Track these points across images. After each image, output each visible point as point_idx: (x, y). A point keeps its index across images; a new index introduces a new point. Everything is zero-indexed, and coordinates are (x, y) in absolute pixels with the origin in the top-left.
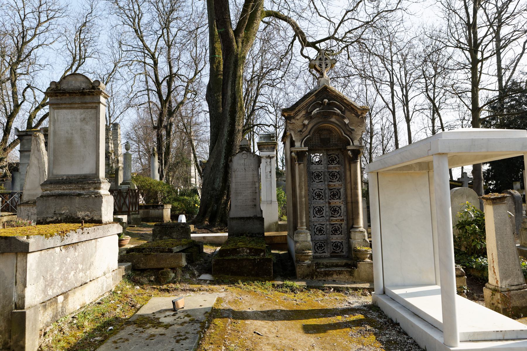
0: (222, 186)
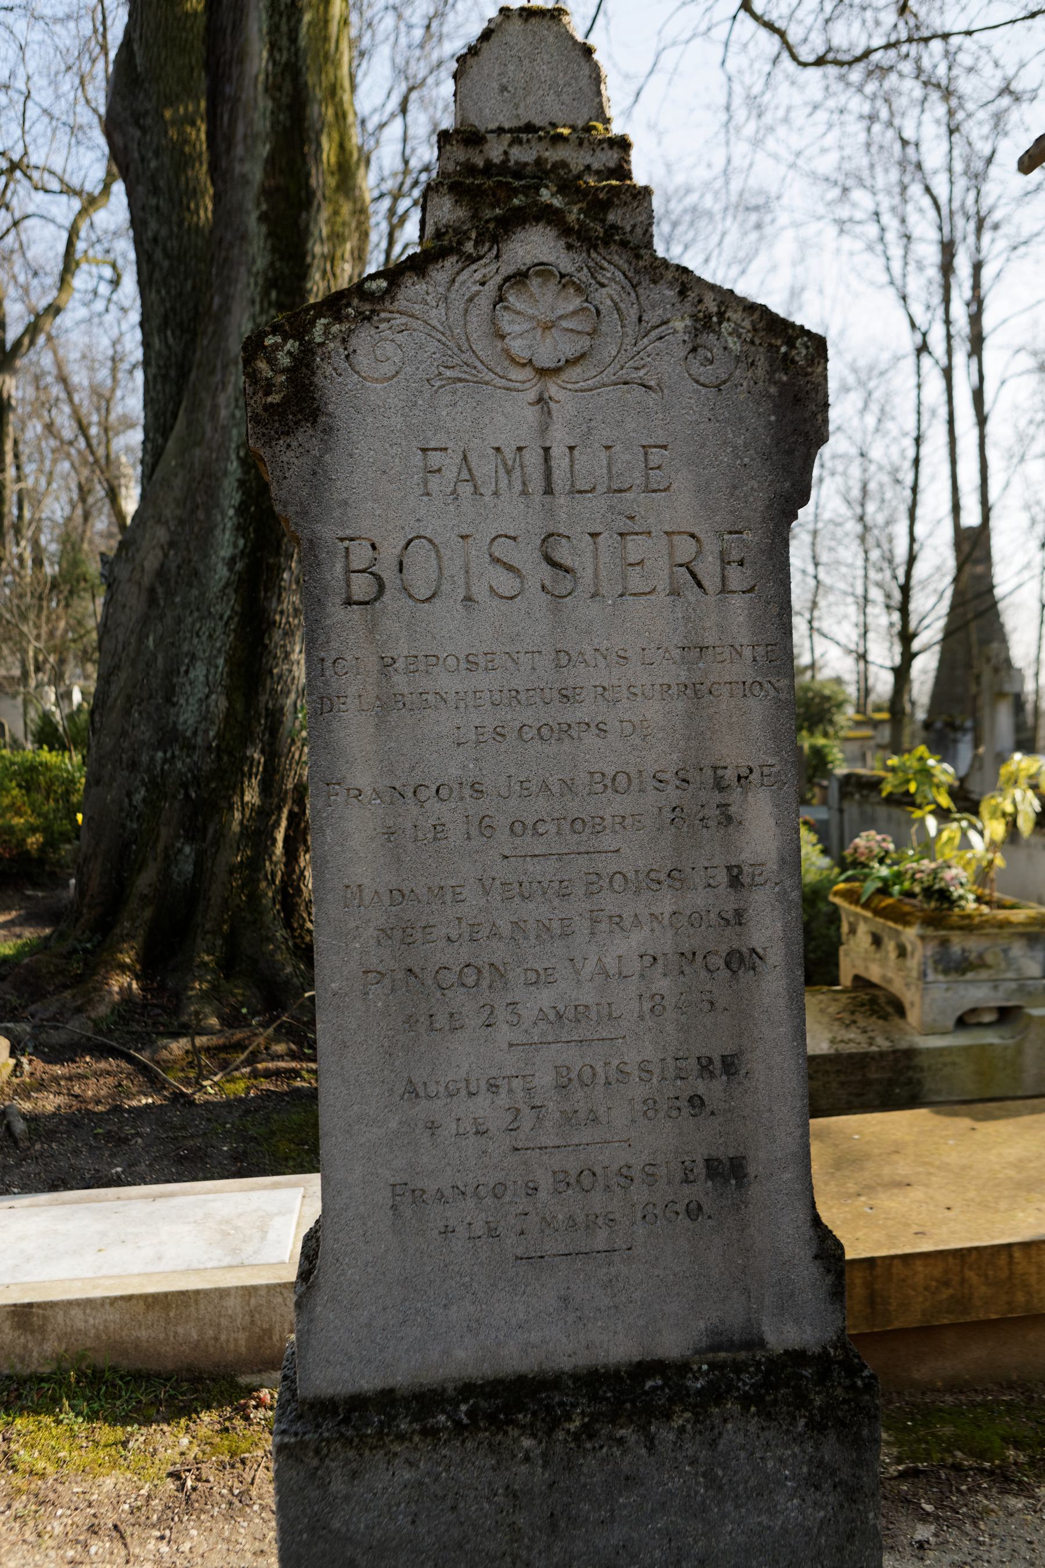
0: (230, 713)
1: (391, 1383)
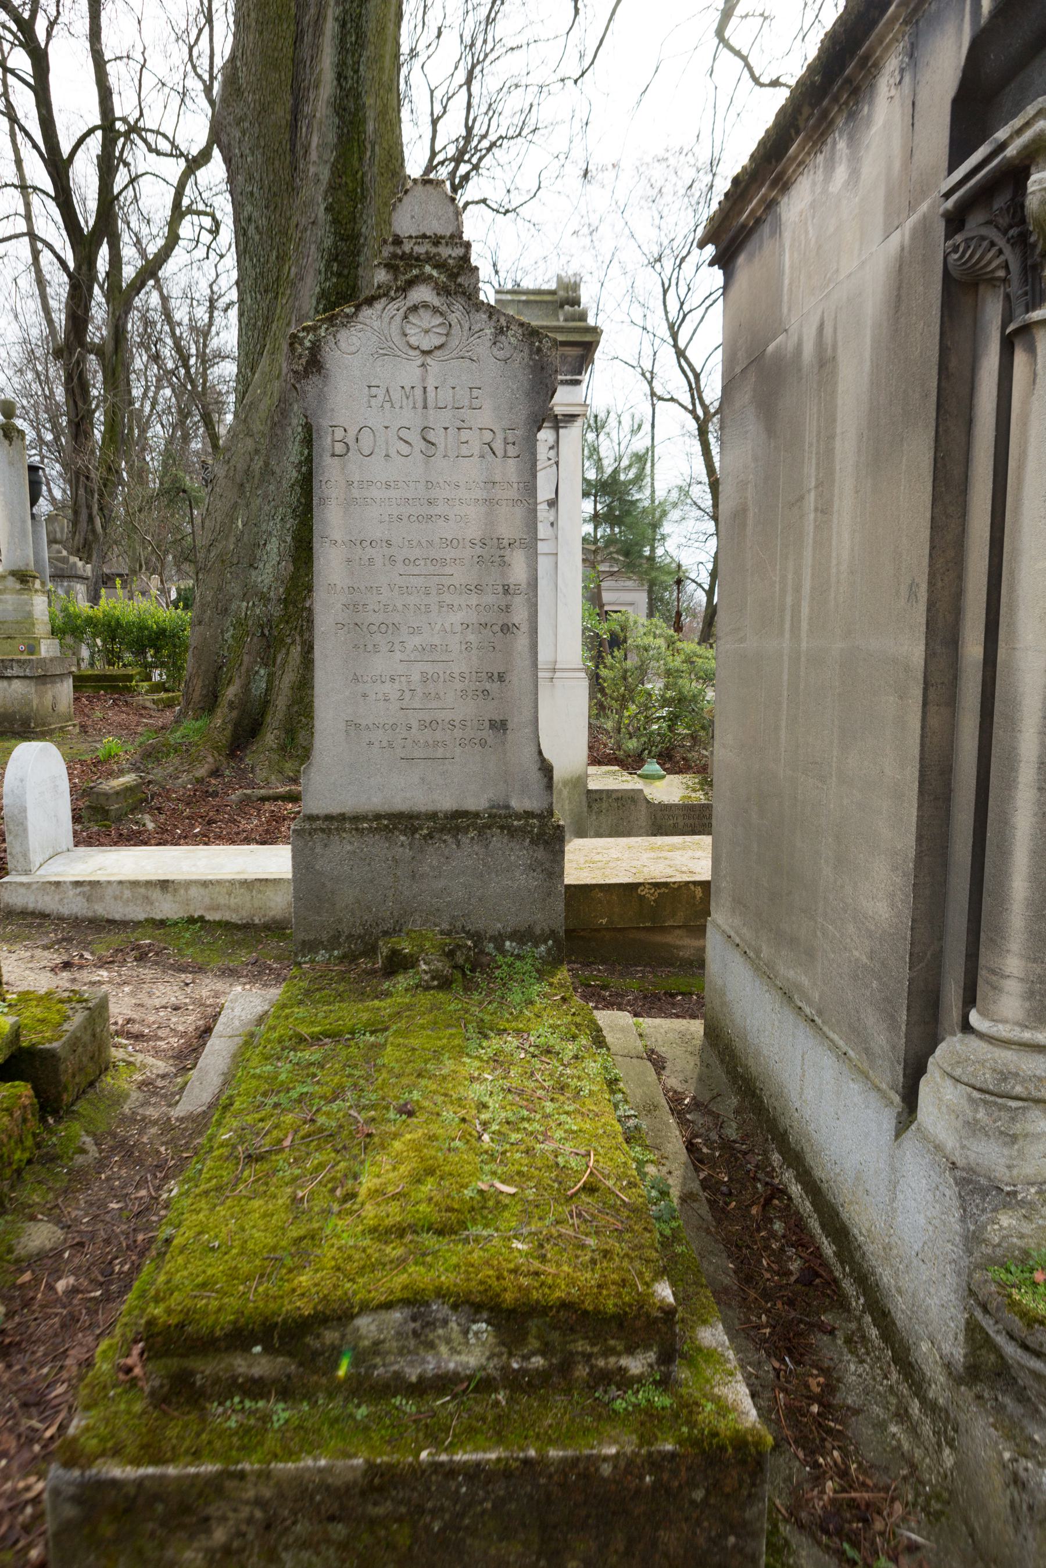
1: (343, 810)
